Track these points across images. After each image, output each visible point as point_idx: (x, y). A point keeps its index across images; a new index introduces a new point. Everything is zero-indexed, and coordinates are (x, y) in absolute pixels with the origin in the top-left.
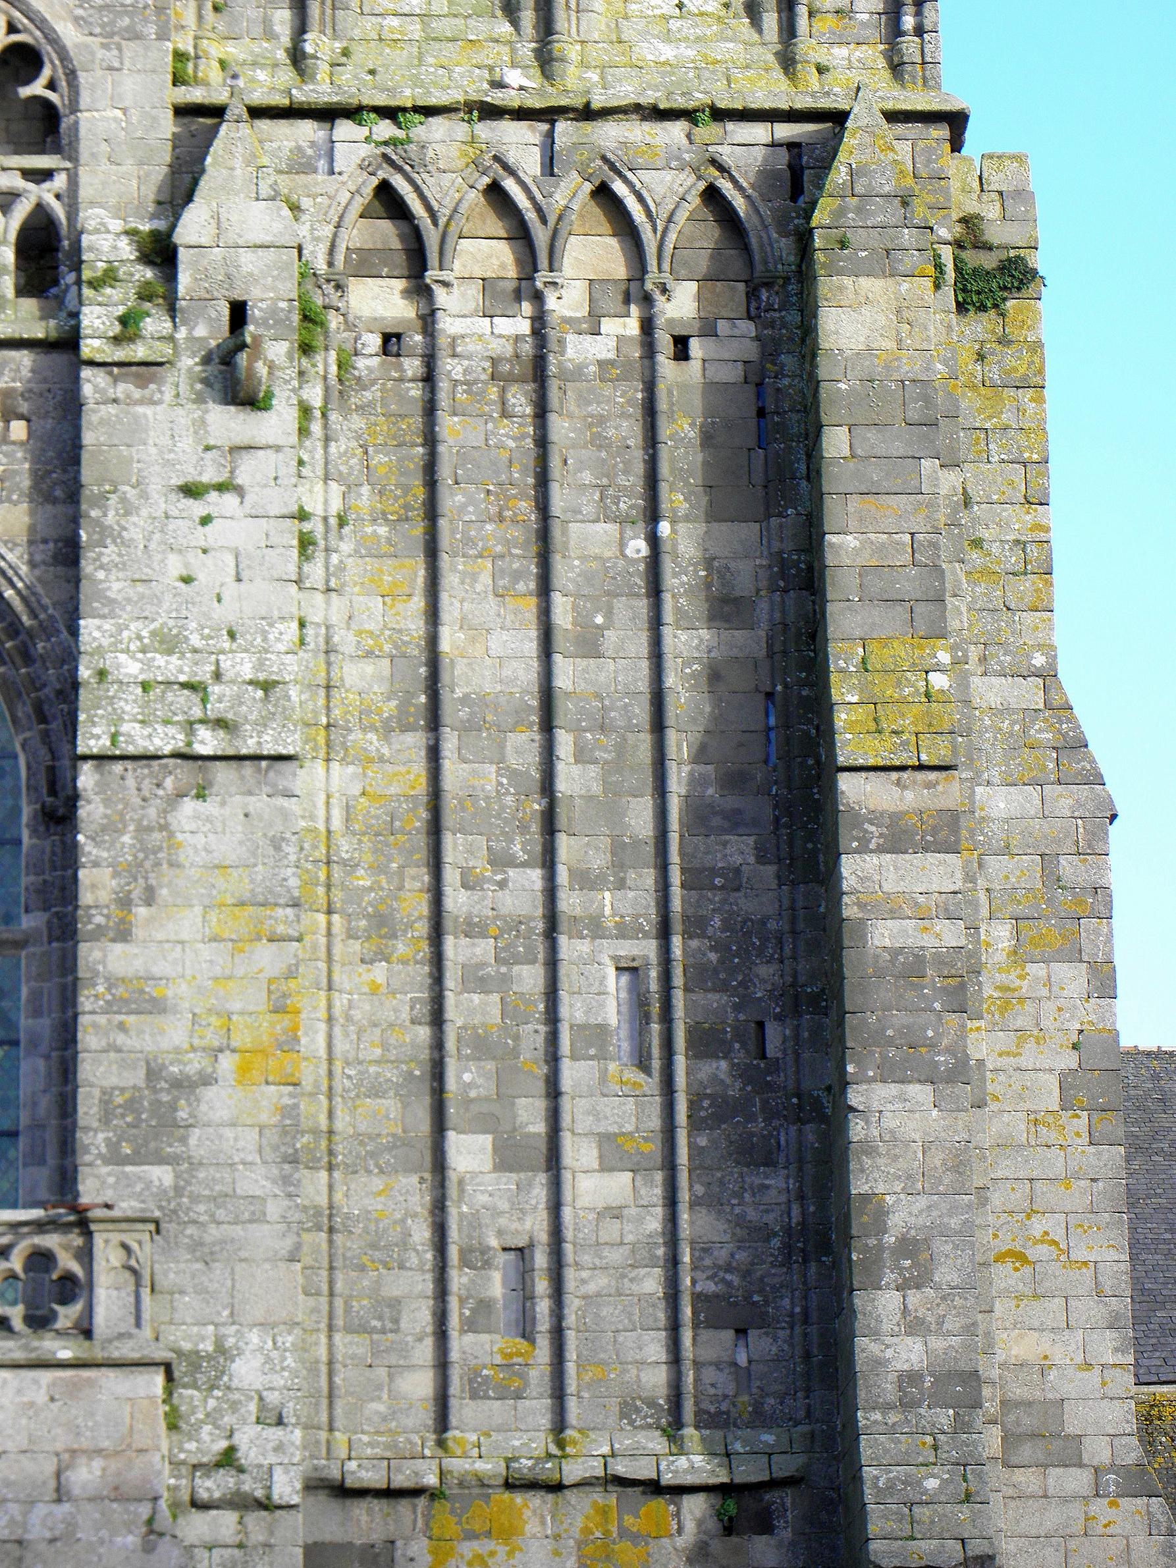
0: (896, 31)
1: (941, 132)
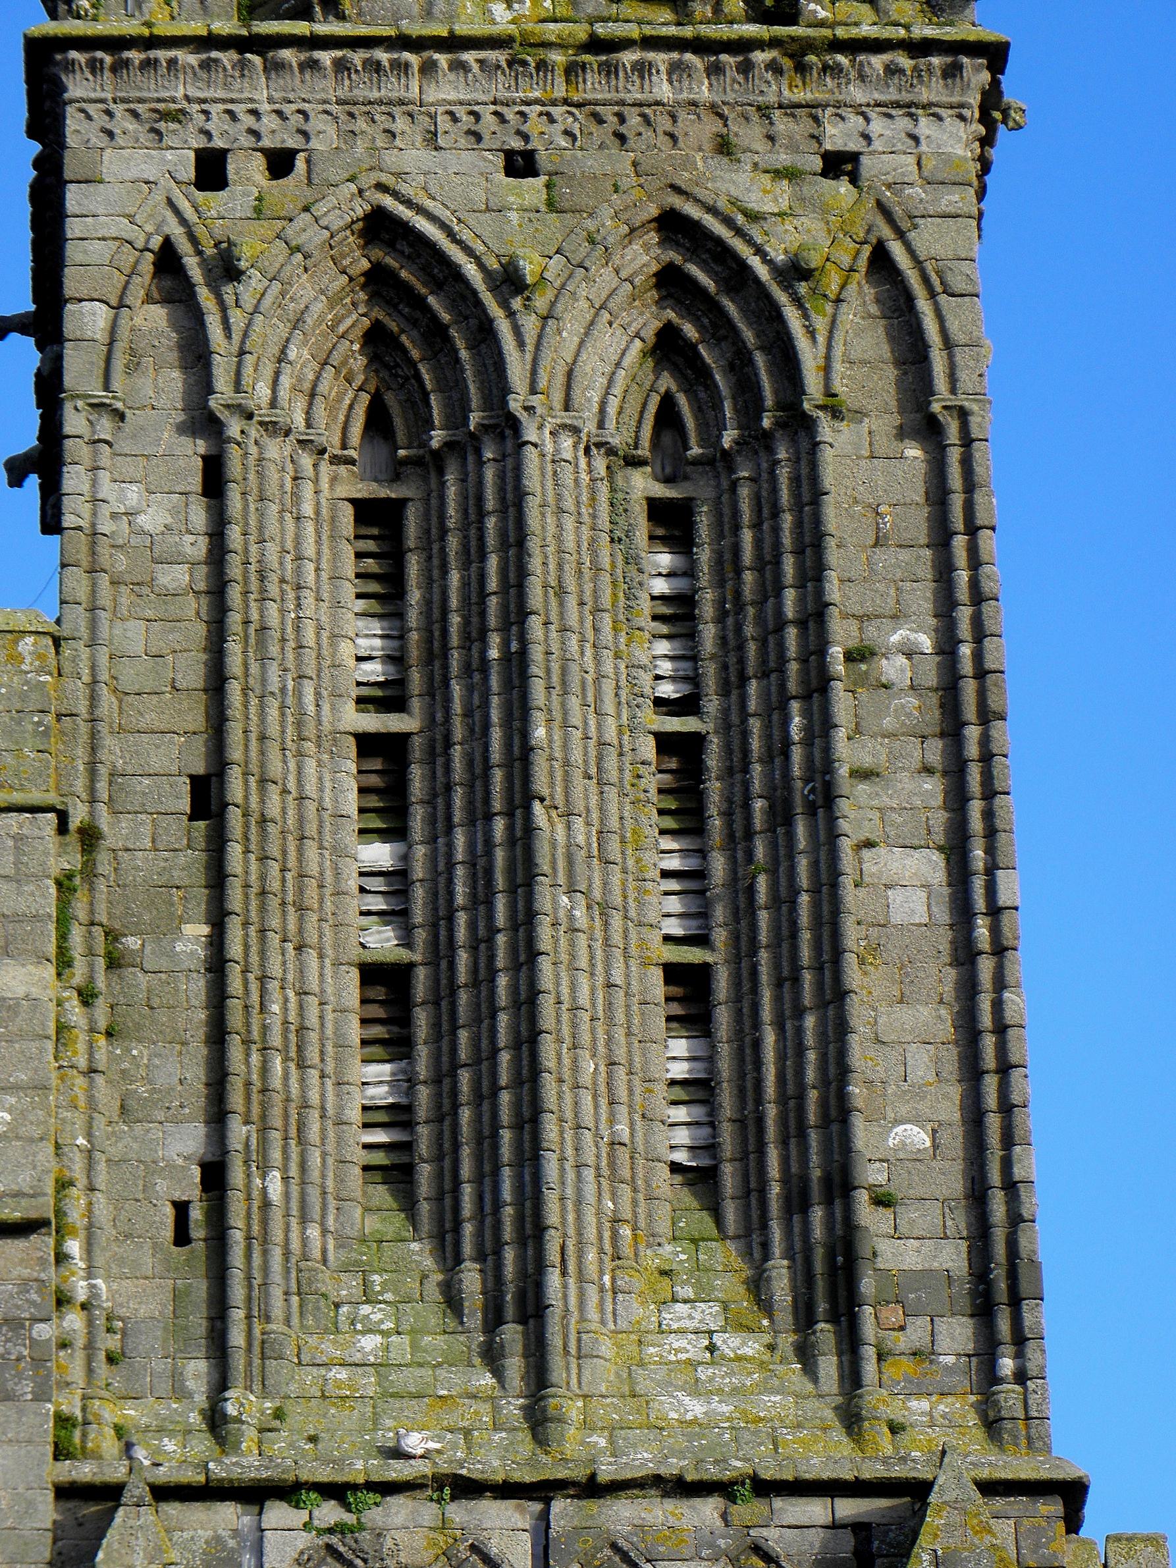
0: (990, 1377)
1: (1053, 1507)
